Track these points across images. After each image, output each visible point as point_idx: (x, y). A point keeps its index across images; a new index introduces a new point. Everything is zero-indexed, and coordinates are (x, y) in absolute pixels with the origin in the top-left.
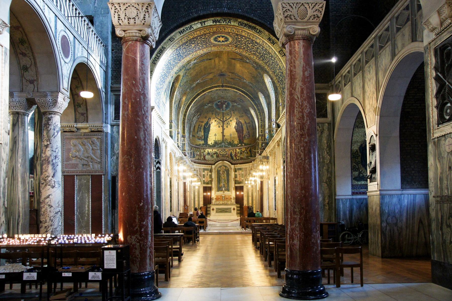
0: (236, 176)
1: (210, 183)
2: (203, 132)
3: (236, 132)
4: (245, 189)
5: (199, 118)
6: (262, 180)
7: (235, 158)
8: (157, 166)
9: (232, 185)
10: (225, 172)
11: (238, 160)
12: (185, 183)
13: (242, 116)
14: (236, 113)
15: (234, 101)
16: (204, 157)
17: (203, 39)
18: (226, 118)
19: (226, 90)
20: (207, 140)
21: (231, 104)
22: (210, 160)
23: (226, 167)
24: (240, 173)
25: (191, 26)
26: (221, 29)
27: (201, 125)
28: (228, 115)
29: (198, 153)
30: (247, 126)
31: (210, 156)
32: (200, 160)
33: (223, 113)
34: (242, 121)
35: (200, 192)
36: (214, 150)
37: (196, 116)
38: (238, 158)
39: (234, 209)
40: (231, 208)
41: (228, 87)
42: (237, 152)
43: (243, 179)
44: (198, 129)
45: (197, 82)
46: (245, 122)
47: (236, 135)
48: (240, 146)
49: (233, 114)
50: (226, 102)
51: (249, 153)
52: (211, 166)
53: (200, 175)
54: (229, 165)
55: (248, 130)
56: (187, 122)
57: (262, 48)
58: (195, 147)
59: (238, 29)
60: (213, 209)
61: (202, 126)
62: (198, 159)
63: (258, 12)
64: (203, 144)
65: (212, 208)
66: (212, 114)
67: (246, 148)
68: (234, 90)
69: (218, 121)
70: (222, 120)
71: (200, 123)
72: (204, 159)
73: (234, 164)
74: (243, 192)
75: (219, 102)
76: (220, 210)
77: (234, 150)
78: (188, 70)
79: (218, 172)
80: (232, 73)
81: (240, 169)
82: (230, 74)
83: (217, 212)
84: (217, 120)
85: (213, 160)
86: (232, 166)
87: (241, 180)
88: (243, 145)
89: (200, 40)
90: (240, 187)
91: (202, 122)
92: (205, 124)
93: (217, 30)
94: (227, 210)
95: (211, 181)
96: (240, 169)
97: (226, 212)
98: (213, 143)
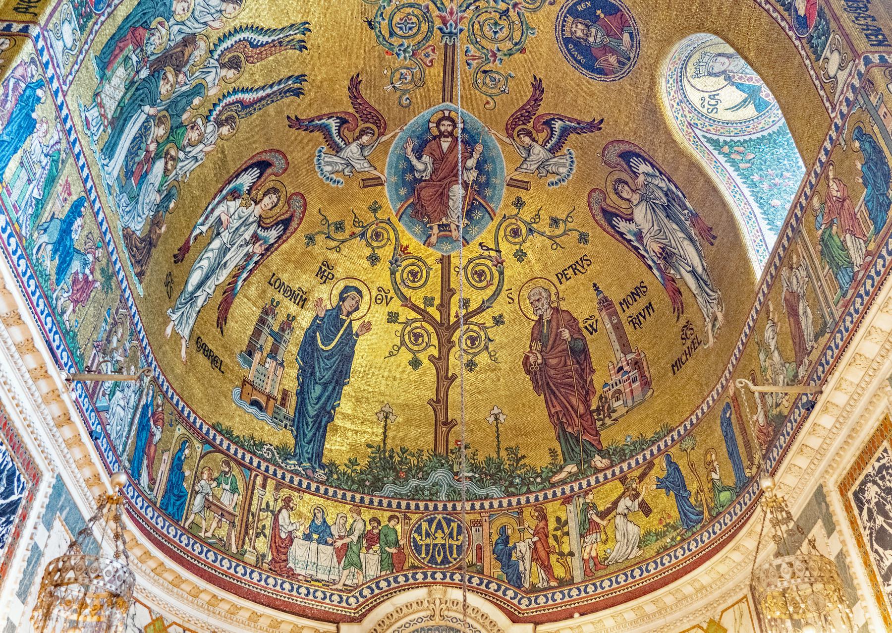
2: (293, 372)
3: (537, 388)
7: (532, 574)
11: (562, 583)
14: (530, 253)
22: (327, 584)
30: (618, 327)
31: (329, 550)
33: (445, 261)
36: (367, 515)
38: (559, 572)
42: (552, 524)
44: (257, 333)
46: (606, 304)
48: (573, 477)
51: (666, 503)
64: (283, 452)
67: (623, 480)
69: (407, 324)
70: (434, 312)
71: (278, 296)
84: (406, 314)
85: (348, 589)
92: (316, 326)
98: (364, 462)
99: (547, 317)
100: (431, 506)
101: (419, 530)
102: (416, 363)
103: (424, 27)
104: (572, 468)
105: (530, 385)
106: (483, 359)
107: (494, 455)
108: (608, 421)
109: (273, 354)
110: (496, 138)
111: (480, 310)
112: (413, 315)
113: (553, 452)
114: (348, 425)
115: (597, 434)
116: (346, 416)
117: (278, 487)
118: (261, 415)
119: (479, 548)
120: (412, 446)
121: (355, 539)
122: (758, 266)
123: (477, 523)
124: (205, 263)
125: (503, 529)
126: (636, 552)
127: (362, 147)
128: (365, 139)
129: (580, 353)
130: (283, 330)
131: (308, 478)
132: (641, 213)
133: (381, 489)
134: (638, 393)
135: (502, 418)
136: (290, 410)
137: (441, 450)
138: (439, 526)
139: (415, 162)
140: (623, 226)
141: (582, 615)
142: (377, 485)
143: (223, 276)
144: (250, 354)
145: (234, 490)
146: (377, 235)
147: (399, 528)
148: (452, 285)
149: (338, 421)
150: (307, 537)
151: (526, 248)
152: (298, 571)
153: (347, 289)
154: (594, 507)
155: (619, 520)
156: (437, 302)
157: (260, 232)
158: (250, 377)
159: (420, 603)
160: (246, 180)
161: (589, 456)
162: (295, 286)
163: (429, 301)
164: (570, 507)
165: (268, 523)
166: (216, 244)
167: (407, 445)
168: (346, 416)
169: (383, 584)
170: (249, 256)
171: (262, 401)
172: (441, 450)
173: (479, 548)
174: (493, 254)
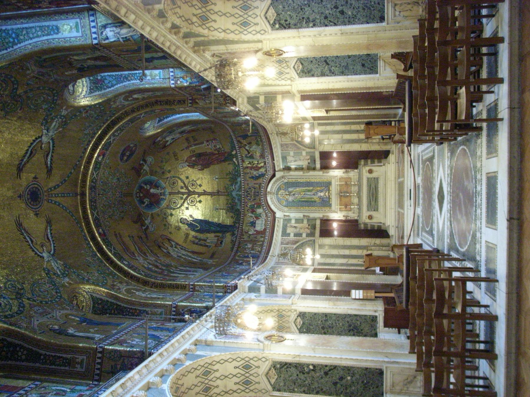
0: (300, 169)
1: (313, 223)
2: (208, 235)
4: (326, 148)
5: (177, 244)
6: (298, 96)
7: (262, 170)
9: (317, 175)
10: (290, 189)
11: (265, 164)
12: (305, 292)
13: (175, 155)
14: (169, 168)
15: (138, 171)
16: (258, 232)
18: (182, 188)
19: (92, 188)
21: (147, 177)
22: (266, 221)
23: (279, 189)
27: (194, 239)
28: (174, 183)
29: (250, 246)
30: (195, 145)
31: (257, 222)
32: (263, 242)
33: (170, 194)
34: (186, 154)
35: (332, 244)
36: (246, 212)
38: (262, 164)
39: (370, 172)
40: (368, 179)
41: (84, 181)
42: (250, 165)
43: (304, 153)
44: (201, 245)
46: (187, 148)
47: (216, 167)
48: (237, 159)
50: (141, 188)
52: (277, 219)
54: (276, 181)
55: (202, 143)
60: (370, 217)
61: (196, 237)
62: (262, 246)
64: (233, 234)
65: (367, 221)
66: (172, 215)
67: (240, 147)
68: (91, 167)
69: (188, 204)
70: (185, 196)
71: (188, 241)
72: (263, 232)
73: (275, 171)
74: (331, 153)
76: (373, 203)
79: (290, 205)
81: (284, 158)
83: (376, 209)
84: (186, 205)
85: (267, 216)
86: (278, 175)
87: (308, 157)
88: (234, 153)
90: (321, 158)
91: (187, 235)
94: (373, 186)
95: (309, 219)
96: (284, 158)
97: (376, 188)
98: (232, 214)
99: (188, 164)
100: (243, 196)
101: (250, 199)
102: (200, 202)
103: (121, 202)
104: (234, 160)
106: (199, 182)
108: (223, 149)
109: (205, 240)
113: (229, 164)
114: (221, 219)
115: (226, 152)
117: (243, 235)
118: (224, 241)
119: (255, 184)
120: (225, 202)
121: (253, 215)
122: (205, 118)
123: (248, 184)
124: (190, 259)
125: (250, 178)
126: (260, 147)
127: (145, 219)
128: (144, 219)
129: (200, 155)
130: (197, 239)
132: (167, 139)
133: (239, 210)
134: (216, 141)
135: (217, 177)
136: (220, 235)
137: (226, 194)
138: (249, 194)
139: (146, 204)
140: (168, 143)
141: (274, 160)
143: (189, 254)
144: (207, 246)
145: (247, 245)
146: (165, 214)
147: (250, 204)
149: (220, 222)
150: (255, 227)
151: (167, 170)
153: (181, 222)
154: (246, 155)
155: (251, 149)
156: (182, 196)
157: (174, 246)
158: (214, 245)
160: (165, 251)
162: (184, 237)
163: (182, 198)
164: (246, 160)
165: (253, 236)
166: (183, 256)
167: (225, 203)
168: (219, 220)
169: (265, 208)
170: (182, 249)
172: (226, 194)
173: (255, 184)
174: (169, 179)
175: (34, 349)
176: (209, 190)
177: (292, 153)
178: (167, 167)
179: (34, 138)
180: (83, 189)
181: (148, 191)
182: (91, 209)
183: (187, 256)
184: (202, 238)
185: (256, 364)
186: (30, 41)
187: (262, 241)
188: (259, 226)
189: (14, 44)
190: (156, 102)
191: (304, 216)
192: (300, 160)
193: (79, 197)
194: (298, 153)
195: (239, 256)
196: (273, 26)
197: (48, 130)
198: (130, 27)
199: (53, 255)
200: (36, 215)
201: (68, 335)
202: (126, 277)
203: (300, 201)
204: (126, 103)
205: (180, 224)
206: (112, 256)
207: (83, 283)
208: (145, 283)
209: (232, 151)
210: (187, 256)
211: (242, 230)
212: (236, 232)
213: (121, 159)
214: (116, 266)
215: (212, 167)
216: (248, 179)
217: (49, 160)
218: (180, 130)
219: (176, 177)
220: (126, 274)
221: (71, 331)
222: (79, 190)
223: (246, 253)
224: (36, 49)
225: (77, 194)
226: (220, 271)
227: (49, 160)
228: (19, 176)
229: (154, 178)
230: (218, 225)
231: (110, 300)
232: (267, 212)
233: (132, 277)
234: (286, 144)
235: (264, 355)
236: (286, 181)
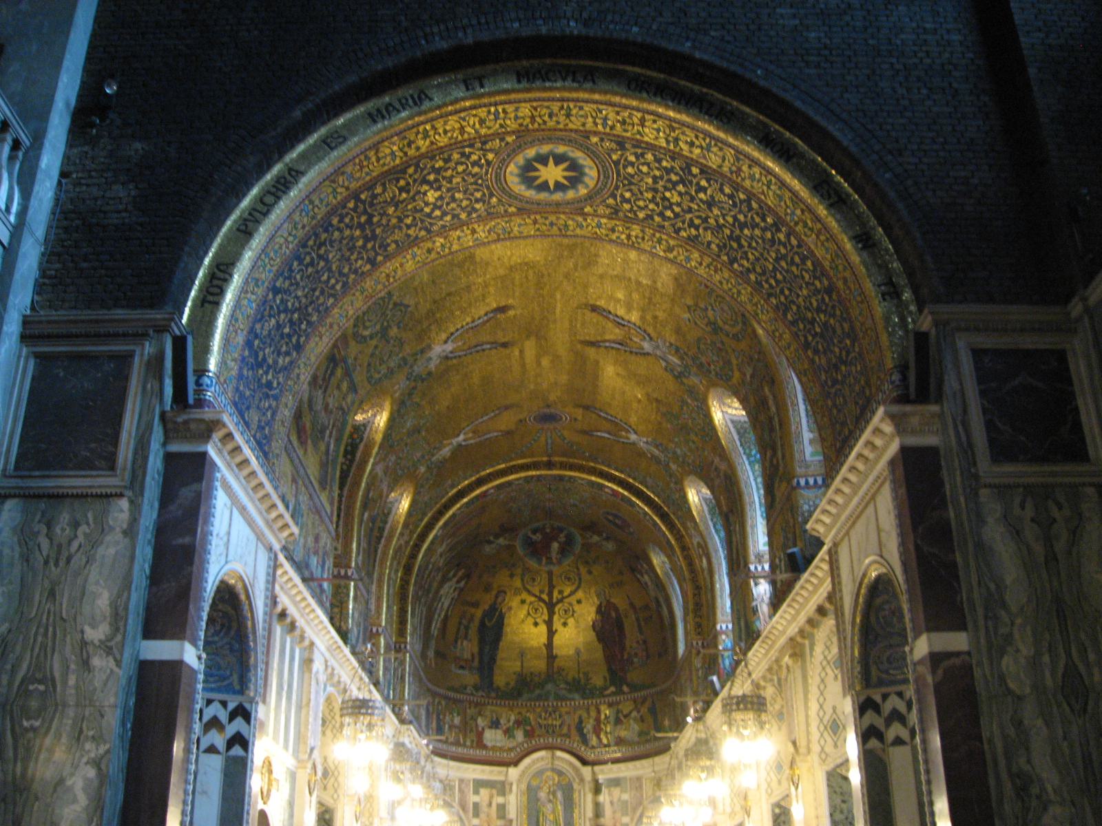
2: (476, 642)
7: (594, 741)
8: (231, 730)
10: (559, 795)
11: (605, 746)
13: (620, 584)
14: (595, 573)
16: (480, 735)
17: (474, 164)
18: (561, 592)
19: (561, 478)
20: (491, 670)
23: (560, 773)
24: (615, 800)
25: (422, 92)
26: (551, 116)
28: (569, 579)
29: (457, 721)
30: (638, 620)
31: (499, 732)
32: (464, 745)
33: (550, 574)
34: (619, 601)
36: (517, 711)
37: (450, 580)
38: (605, 741)
41: (572, 467)
43: (626, 820)
44: (458, 629)
45: (455, 441)
46: (632, 605)
48: (613, 694)
49: (585, 576)
50: (561, 530)
52: (503, 769)
53: (463, 807)
54: (574, 767)
55: (641, 632)
56: (417, 598)
57: (731, 197)
58: (446, 698)
59: (626, 107)
61: (471, 619)
62: (457, 743)
63: (713, 33)
64: (476, 688)
66: (512, 576)
67: (635, 701)
68: (593, 478)
69: (531, 603)
70: (545, 597)
72: (480, 744)
73: (593, 763)
75: (535, 532)
77: (593, 709)
78: (423, 380)
79: (531, 793)
80: (587, 408)
81: (616, 782)
82: (579, 413)
85: (510, 750)
86: (586, 771)
88: (625, 688)
89: (460, 168)
91: (476, 605)
93: (533, 118)
96: (616, 782)
98: (512, 683)
101: (540, 717)
105: (595, 639)
107: (577, 676)
110: (573, 530)
111: (569, 595)
112: (533, 599)
113: (605, 678)
116: (502, 659)
117: (475, 707)
118: (466, 672)
119: (569, 726)
121: (511, 724)
123: (568, 713)
124: (436, 616)
125: (580, 717)
126: (636, 739)
130: (469, 623)
131: (489, 697)
132: (646, 578)
136: (476, 663)
138: (550, 714)
140: (639, 576)
142: (520, 695)
143: (443, 613)
145: (458, 714)
146: (514, 565)
148: (554, 583)
149: (498, 662)
150: (490, 727)
152: (489, 744)
153: (499, 592)
155: (631, 721)
156: (546, 590)
159: (542, 758)
160: (452, 573)
161: (621, 686)
163: (542, 592)
165: (474, 725)
168: (502, 659)
169: (525, 745)
171: (462, 663)
173: (569, 726)
175: (349, 479)
176: (557, 640)
177: (625, 797)
178: (597, 569)
179: (634, 427)
180: (558, 466)
181: (555, 538)
182: (526, 477)
183: (441, 611)
184: (470, 632)
185: (330, 786)
186: (752, 478)
187: (465, 742)
188: (492, 737)
189: (749, 456)
190: (698, 588)
191: (511, 821)
192: (614, 812)
193: (545, 459)
194: (627, 807)
195: (439, 703)
196: (778, 805)
197: (647, 443)
198: (771, 616)
199: (460, 445)
200: (521, 421)
201: (363, 515)
202: (419, 535)
203: (538, 812)
204: (695, 543)
205: (494, 593)
206: (450, 512)
207: (416, 489)
208: (408, 569)
209: (628, 685)
210: (441, 611)
211: (484, 704)
212: (480, 693)
213: (608, 513)
214: (435, 519)
215: (600, 647)
216: (579, 712)
217: (604, 435)
218: (661, 600)
219: (580, 583)
220: (423, 537)
221: (366, 515)
222: (556, 459)
223: (445, 716)
224: (743, 485)
225: (549, 456)
226: (420, 680)
227: (604, 435)
228: (577, 406)
229: (578, 549)
230: (493, 659)
231: (388, 526)
232: (518, 750)
233: (417, 547)
234: (641, 787)
235: (341, 797)
236: (576, 786)
